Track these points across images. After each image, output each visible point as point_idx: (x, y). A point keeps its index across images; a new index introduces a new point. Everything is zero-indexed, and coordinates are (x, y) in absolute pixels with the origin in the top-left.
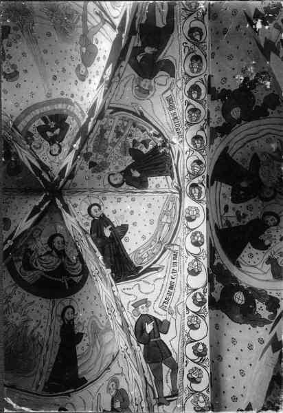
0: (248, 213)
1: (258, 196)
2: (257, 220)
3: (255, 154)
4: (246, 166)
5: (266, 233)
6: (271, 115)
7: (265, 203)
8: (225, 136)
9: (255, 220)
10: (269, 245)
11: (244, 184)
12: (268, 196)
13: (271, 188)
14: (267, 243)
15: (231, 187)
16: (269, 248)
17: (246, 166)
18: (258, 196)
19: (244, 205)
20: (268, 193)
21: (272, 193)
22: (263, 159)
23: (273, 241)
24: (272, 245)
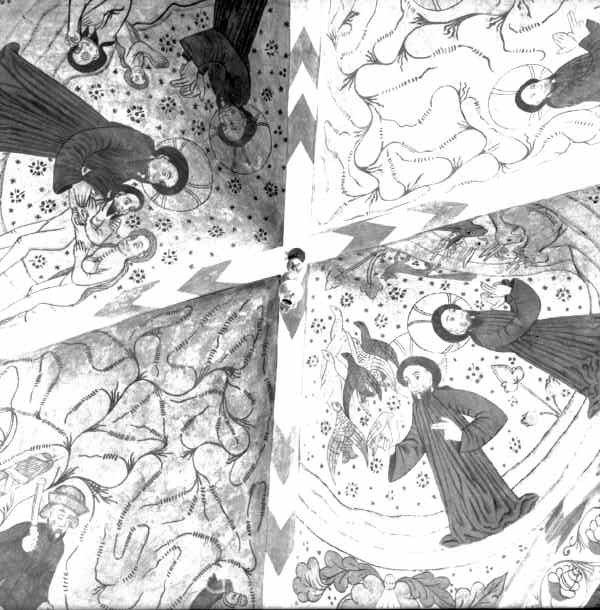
0: (485, 368)
1: (441, 385)
2: (478, 342)
3: (392, 476)
4: (424, 466)
5: (487, 308)
6: (325, 548)
7: (436, 358)
8: (437, 574)
9: (480, 344)
10: (504, 282)
11: (452, 432)
12: (421, 369)
13: (405, 384)
14: (507, 290)
15: (486, 449)
16: (510, 279)
17: (424, 466)
18: (441, 385)
19: (481, 390)
20: (422, 380)
21: (409, 372)
22: (384, 456)
23: (490, 284)
24: (501, 279)
